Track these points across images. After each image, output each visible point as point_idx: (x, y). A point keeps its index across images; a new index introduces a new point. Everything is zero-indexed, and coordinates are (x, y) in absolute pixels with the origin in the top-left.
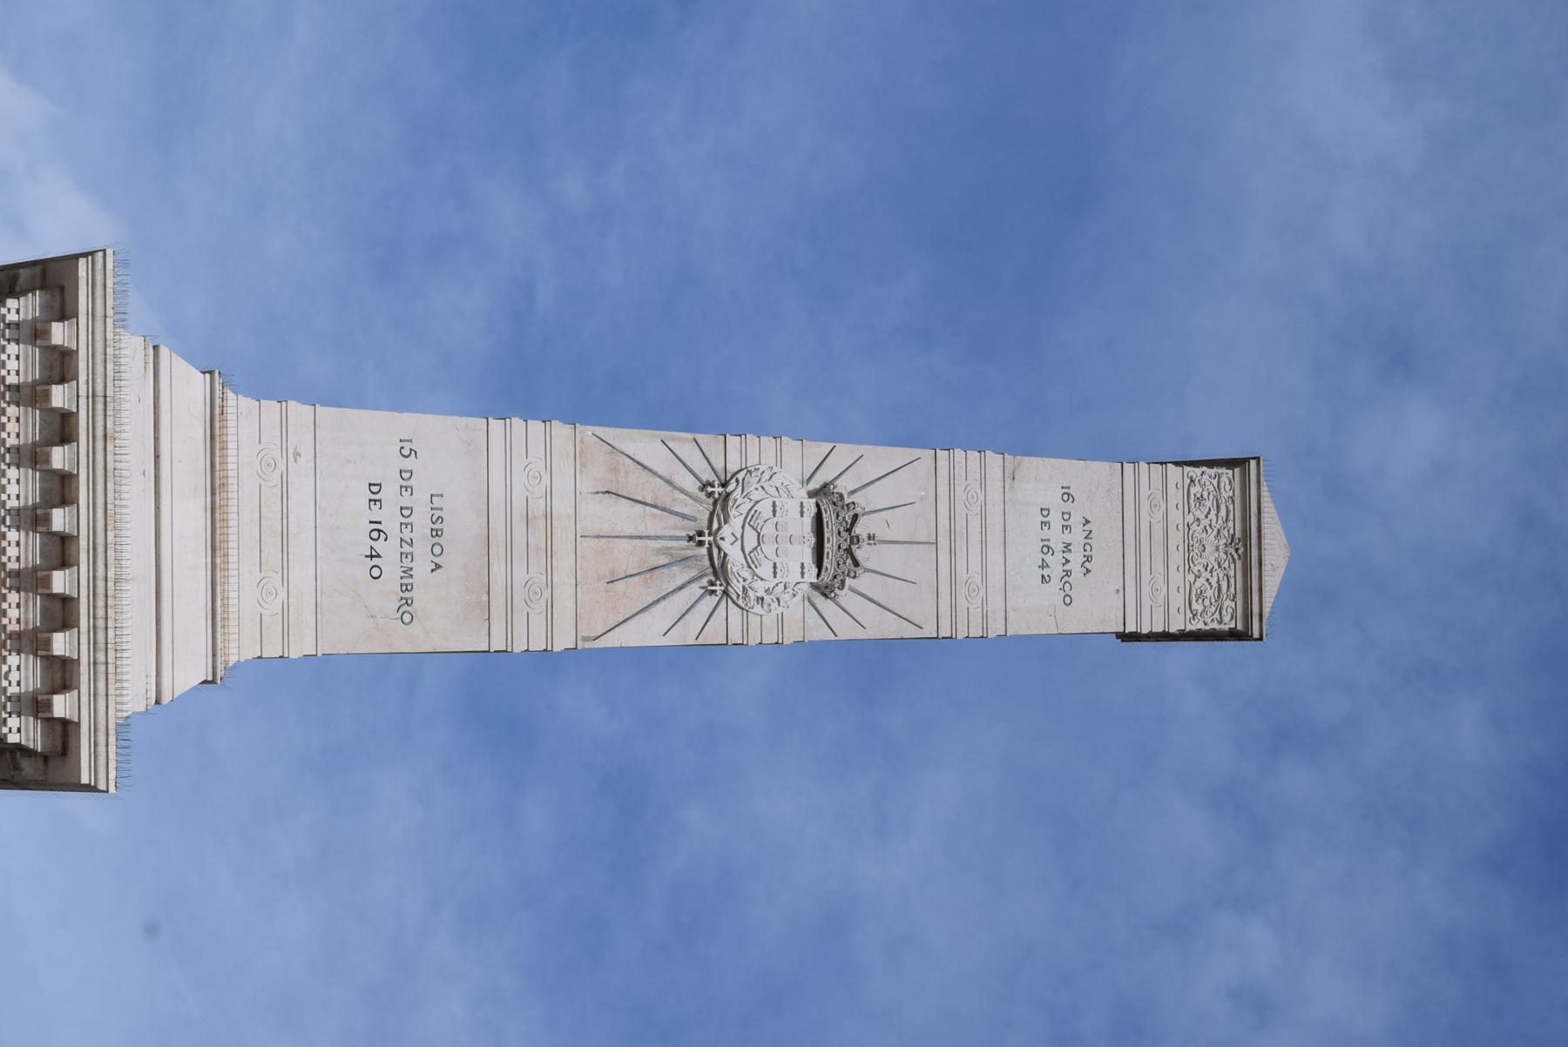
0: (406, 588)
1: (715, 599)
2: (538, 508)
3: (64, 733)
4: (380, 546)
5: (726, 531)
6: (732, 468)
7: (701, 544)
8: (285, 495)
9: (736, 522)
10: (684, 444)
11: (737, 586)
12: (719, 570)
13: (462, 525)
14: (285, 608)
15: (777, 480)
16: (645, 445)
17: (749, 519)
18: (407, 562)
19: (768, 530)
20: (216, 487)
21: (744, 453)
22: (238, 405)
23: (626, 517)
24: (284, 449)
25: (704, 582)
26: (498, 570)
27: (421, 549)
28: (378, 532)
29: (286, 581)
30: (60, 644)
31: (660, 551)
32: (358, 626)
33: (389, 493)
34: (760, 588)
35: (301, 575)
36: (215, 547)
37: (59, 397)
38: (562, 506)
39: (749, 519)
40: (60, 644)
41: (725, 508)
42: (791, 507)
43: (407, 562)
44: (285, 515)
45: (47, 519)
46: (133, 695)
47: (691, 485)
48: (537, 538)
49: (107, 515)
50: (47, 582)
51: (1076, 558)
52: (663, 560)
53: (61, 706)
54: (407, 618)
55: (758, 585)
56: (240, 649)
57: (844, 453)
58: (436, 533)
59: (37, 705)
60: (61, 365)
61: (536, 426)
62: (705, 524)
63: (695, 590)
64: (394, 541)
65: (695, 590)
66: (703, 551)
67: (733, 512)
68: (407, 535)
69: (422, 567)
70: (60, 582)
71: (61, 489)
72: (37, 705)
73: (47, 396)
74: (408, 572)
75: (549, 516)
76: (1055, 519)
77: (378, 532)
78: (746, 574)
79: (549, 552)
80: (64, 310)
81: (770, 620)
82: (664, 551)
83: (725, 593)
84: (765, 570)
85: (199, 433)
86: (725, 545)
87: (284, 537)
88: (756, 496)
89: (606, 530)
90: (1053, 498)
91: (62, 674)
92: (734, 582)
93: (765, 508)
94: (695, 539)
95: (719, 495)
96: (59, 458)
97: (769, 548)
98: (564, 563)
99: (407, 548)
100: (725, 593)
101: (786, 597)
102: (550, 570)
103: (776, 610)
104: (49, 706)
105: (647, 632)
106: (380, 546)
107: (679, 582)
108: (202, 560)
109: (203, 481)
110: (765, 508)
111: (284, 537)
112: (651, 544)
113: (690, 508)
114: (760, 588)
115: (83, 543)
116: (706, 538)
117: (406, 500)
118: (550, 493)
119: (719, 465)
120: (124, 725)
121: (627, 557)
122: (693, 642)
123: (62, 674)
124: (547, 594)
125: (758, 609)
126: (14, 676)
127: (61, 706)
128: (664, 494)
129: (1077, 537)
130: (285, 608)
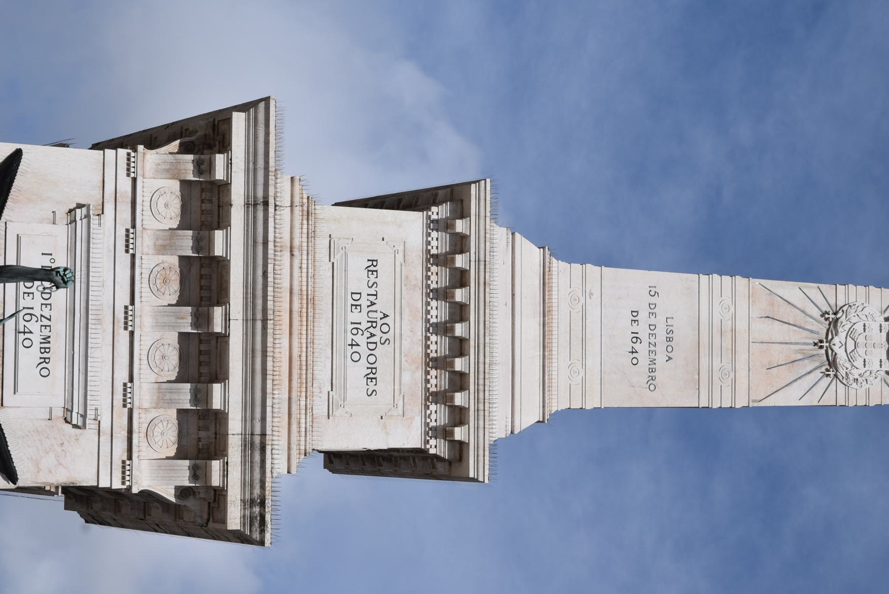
0: (652, 370)
1: (829, 379)
2: (728, 325)
3: (460, 448)
4: (637, 346)
5: (836, 340)
6: (840, 304)
7: (821, 347)
8: (584, 318)
9: (842, 335)
10: (812, 289)
11: (842, 372)
12: (832, 363)
13: (684, 335)
14: (584, 381)
15: (866, 311)
16: (789, 290)
17: (850, 333)
18: (652, 356)
19: (861, 340)
20: (545, 313)
21: (847, 295)
22: (559, 267)
23: (778, 331)
24: (584, 292)
25: (823, 369)
26: (704, 361)
27: (661, 349)
28: (636, 339)
29: (584, 365)
30: (459, 399)
31: (798, 351)
32: (625, 392)
33: (643, 316)
34: (855, 373)
35: (593, 362)
37: (460, 261)
38: (741, 325)
39: (850, 333)
40: (459, 399)
41: (835, 327)
42: (874, 327)
43: (652, 356)
44: (584, 328)
45: (452, 329)
46: (499, 430)
47: (816, 313)
48: (727, 343)
49: (485, 326)
50: (452, 364)
52: (799, 356)
53: (459, 434)
54: (652, 387)
55: (855, 371)
56: (558, 404)
58: (669, 339)
59: (444, 433)
60: (460, 244)
61: (727, 279)
62: (823, 337)
63: (818, 374)
64: (645, 344)
65: (818, 374)
66: (823, 351)
67: (840, 329)
68: (652, 340)
69: (661, 358)
70: (459, 364)
71: (460, 312)
72: (444, 433)
73: (453, 261)
74: (653, 361)
75: (734, 331)
77: (636, 339)
78: (848, 365)
79: (734, 351)
80: (462, 213)
81: (862, 392)
82: (800, 351)
83: (836, 376)
84: (859, 363)
85: (536, 282)
86: (836, 348)
87: (584, 341)
88: (854, 320)
89: (766, 339)
91: (459, 416)
92: (840, 370)
93: (859, 327)
94: (818, 344)
96: (459, 295)
97: (861, 350)
98: (742, 358)
99: (652, 348)
100: (836, 376)
101: (871, 379)
102: (734, 361)
103: (865, 386)
104: (452, 433)
105: (790, 398)
106: (637, 346)
107: (809, 370)
108: (537, 353)
109: (538, 308)
110: (859, 327)
111: (584, 341)
112: (793, 347)
113: (815, 326)
114: (855, 373)
115: (472, 343)
116: (825, 344)
117: (652, 321)
118: (734, 317)
119: (832, 302)
120: (494, 446)
121: (779, 354)
122: (816, 403)
123: (459, 416)
124: (732, 375)
125: (854, 385)
126: (433, 417)
127: (459, 434)
128: (800, 318)
130: (584, 381)
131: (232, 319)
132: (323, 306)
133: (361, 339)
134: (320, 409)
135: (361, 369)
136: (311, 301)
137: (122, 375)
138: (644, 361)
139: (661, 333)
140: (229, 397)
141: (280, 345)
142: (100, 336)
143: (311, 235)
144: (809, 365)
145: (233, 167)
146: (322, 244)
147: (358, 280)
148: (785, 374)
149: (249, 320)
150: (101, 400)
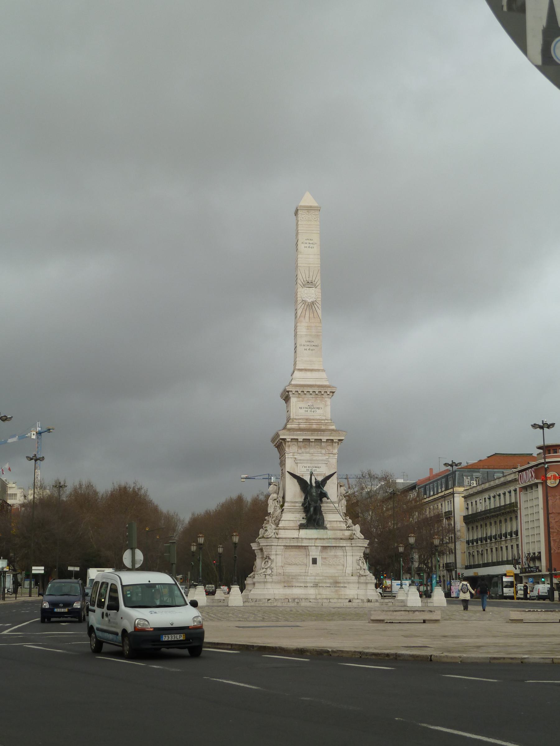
9: (307, 300)
12: (313, 303)
20: (306, 370)
23: (307, 315)
26: (313, 334)
28: (309, 349)
33: (305, 348)
36: (312, 370)
51: (311, 242)
57: (299, 281)
69: (313, 344)
76: (306, 245)
77: (309, 349)
84: (313, 296)
90: (303, 245)
95: (304, 302)
121: (312, 315)
129: (308, 241)
131: (312, 438)
132: (307, 417)
133: (313, 410)
134: (324, 418)
135: (317, 410)
136: (307, 419)
137: (320, 455)
138: (314, 348)
139: (308, 343)
140: (324, 439)
141: (314, 427)
142: (315, 458)
143: (296, 419)
144: (313, 308)
145: (288, 438)
146: (297, 417)
147: (302, 411)
148: (315, 313)
149: (312, 435)
150: (324, 458)
